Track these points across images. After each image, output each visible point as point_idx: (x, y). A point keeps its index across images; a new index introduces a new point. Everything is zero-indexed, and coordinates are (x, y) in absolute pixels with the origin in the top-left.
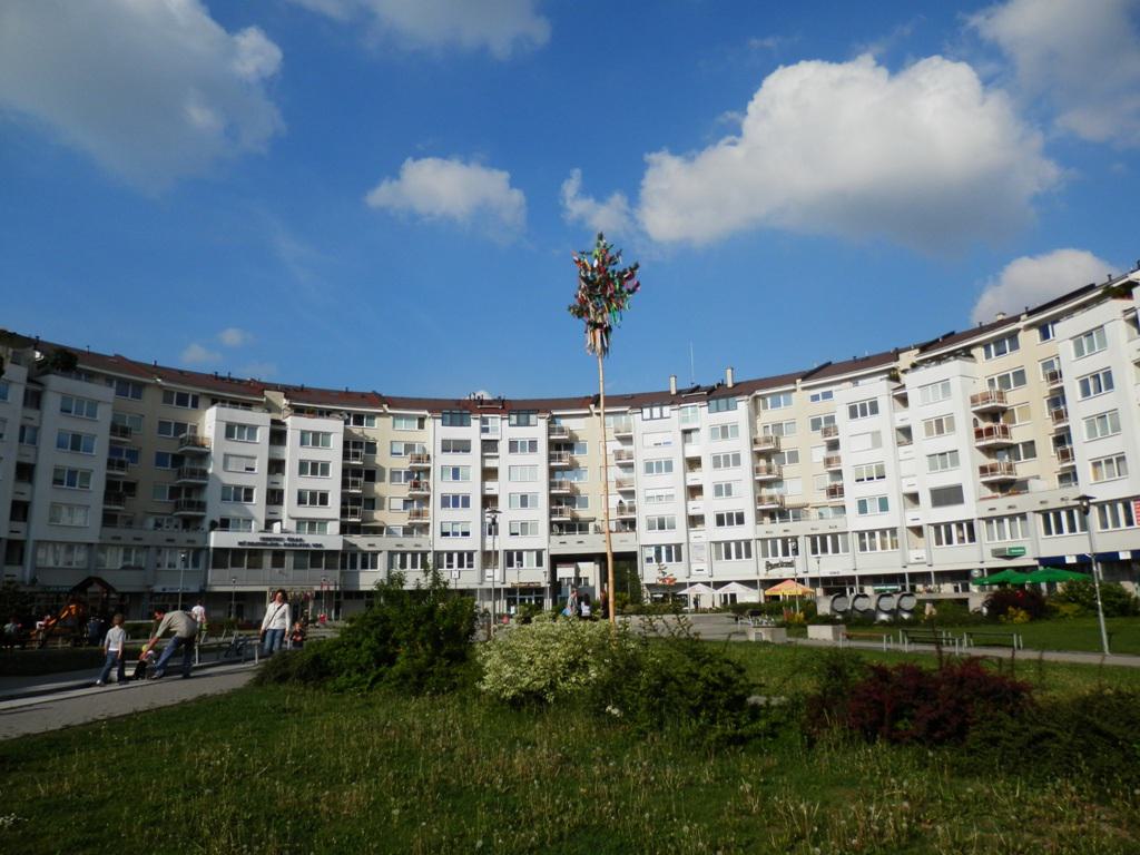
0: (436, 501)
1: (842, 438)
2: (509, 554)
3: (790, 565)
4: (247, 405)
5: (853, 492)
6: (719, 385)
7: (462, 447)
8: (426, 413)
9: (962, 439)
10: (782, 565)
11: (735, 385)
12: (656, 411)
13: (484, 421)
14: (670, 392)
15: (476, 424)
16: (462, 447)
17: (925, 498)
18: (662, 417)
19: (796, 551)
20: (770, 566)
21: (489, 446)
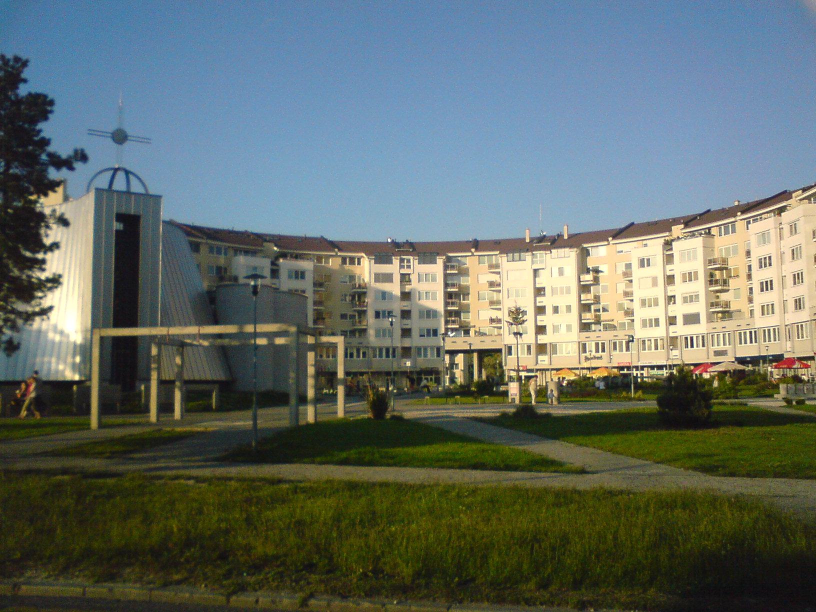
0: (371, 314)
1: (634, 278)
2: (419, 349)
3: (601, 358)
4: (254, 253)
5: (641, 313)
6: (558, 236)
7: (388, 278)
8: (364, 255)
9: (699, 286)
10: (595, 358)
11: (571, 237)
12: (516, 255)
13: (402, 261)
14: (525, 239)
15: (396, 261)
16: (388, 278)
17: (680, 320)
18: (520, 260)
19: (603, 351)
20: (587, 359)
21: (405, 279)
